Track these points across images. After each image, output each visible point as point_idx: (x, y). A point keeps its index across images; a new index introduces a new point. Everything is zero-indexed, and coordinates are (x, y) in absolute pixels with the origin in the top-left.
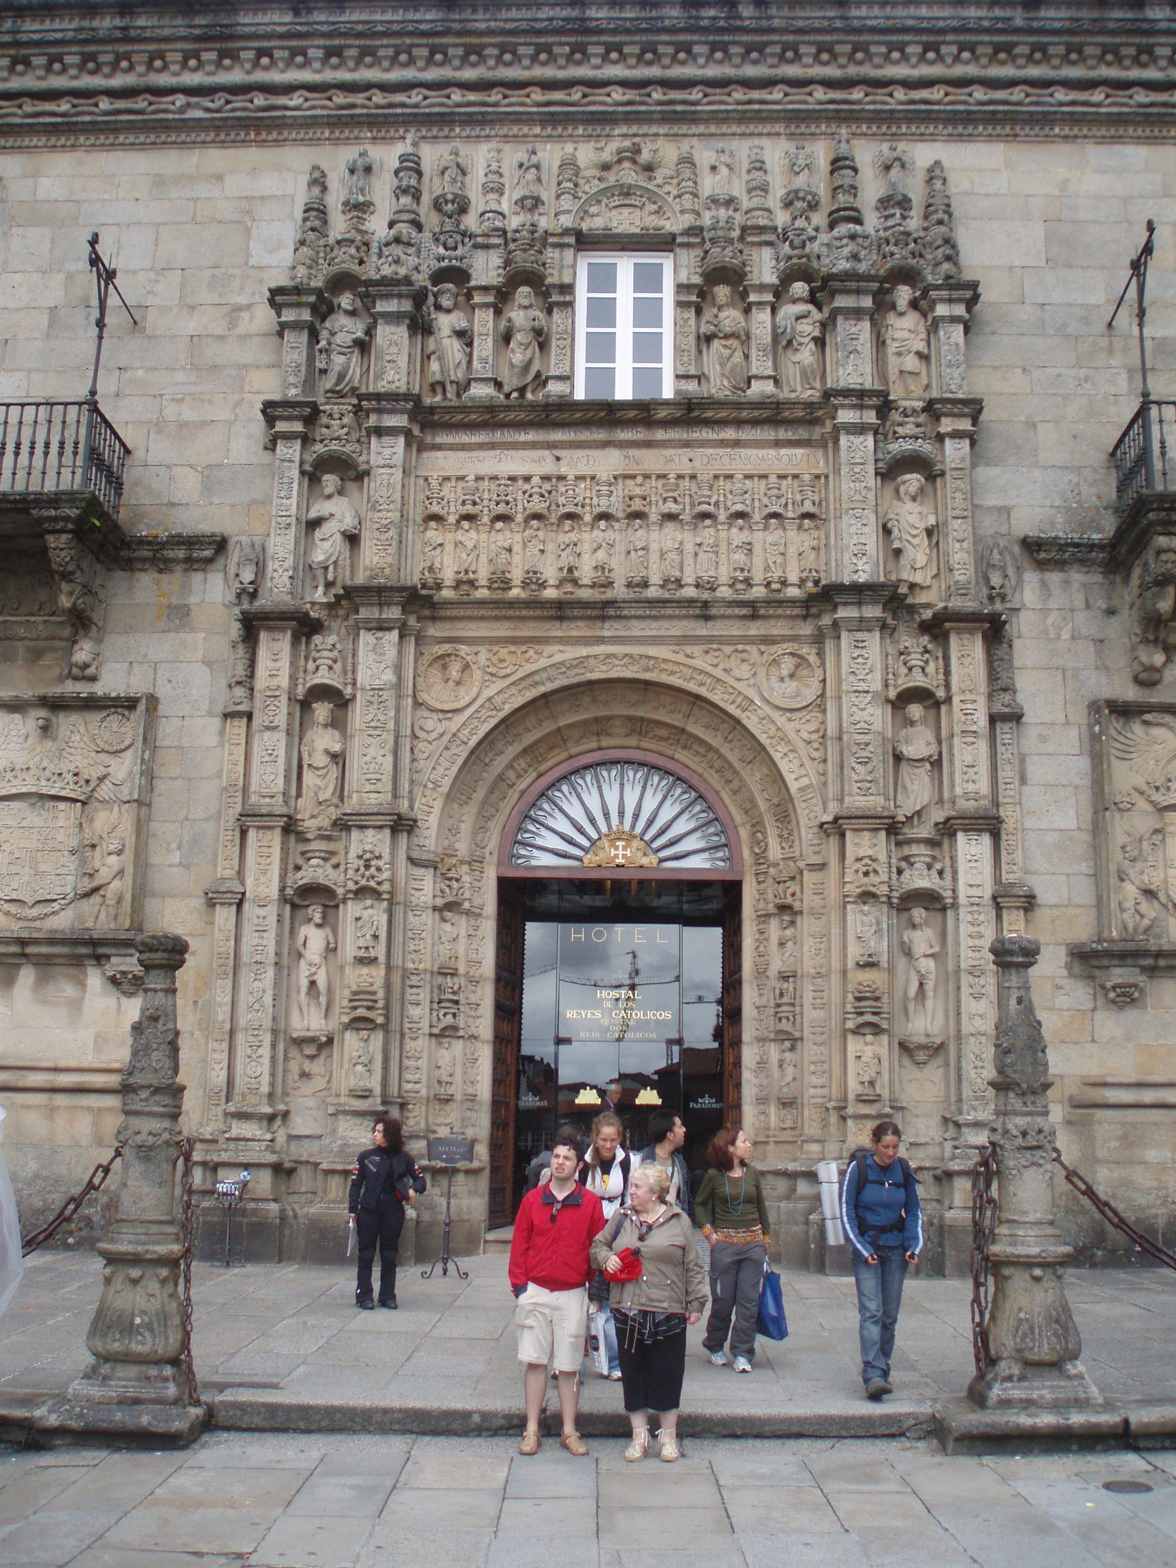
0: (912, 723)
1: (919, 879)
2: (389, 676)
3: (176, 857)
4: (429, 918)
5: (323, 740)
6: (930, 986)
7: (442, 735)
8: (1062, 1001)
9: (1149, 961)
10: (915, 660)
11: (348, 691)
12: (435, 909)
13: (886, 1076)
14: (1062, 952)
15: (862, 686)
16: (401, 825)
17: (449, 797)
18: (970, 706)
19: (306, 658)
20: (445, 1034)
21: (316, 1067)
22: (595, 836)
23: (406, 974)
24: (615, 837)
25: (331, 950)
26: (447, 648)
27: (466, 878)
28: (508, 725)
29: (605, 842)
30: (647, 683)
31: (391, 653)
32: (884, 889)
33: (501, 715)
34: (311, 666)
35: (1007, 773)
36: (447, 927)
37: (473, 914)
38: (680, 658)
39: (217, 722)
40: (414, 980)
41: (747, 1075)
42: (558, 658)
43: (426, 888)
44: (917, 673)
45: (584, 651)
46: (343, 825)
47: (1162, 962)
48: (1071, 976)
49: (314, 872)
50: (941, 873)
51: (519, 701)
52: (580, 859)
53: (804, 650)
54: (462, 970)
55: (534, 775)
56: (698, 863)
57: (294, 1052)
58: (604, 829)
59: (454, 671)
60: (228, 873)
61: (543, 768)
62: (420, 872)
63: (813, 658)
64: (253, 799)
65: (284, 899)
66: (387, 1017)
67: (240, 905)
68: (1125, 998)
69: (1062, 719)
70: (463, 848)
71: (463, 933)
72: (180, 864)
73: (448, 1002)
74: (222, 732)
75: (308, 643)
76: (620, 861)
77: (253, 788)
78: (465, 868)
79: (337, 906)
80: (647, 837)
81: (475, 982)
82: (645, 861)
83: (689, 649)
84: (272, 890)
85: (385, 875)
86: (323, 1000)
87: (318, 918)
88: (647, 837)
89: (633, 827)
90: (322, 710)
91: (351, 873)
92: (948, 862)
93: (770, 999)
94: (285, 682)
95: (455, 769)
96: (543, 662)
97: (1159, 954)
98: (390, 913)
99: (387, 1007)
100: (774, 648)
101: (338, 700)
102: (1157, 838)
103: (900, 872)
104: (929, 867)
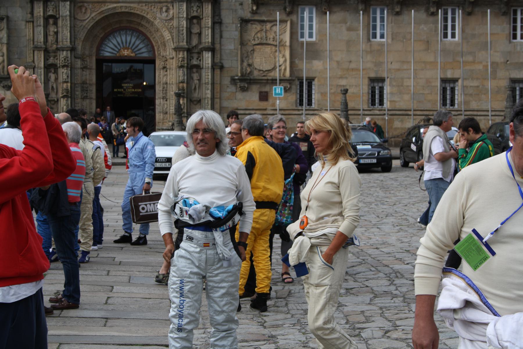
0: (194, 24)
1: (195, 62)
2: (68, 13)
3: (16, 57)
4: (79, 71)
5: (52, 29)
6: (197, 87)
7: (81, 26)
8: (229, 90)
9: (249, 81)
10: (195, 9)
11: (58, 16)
12: (81, 68)
13: (186, 107)
14: (229, 79)
15: (182, 16)
16: (73, 49)
17: (83, 41)
18: (208, 21)
19: (47, 7)
20: (84, 98)
21: (54, 106)
22: (119, 48)
23: (75, 84)
24: (125, 48)
25: (56, 79)
26: (81, 4)
27: (88, 60)
28: (97, 23)
29: (122, 50)
30: (131, 13)
31: (68, 7)
32: (186, 65)
33: (95, 21)
34: (48, 10)
35: (217, 36)
36: (84, 72)
37: (90, 69)
38: (139, 7)
39: (24, 23)
40: (77, 85)
41: (157, 106)
42: (109, 7)
43: (79, 63)
44: (195, 12)
45: (115, 5)
46: (58, 49)
47: (252, 81)
48: (231, 84)
49: (51, 61)
50: (200, 60)
51: (100, 17)
52: (116, 54)
53: (169, 5)
54: (88, 82)
55: (104, 34)
56: (145, 55)
57: (49, 103)
58: (122, 46)
59: (83, 10)
60: (30, 61)
61: (107, 31)
62: (77, 60)
63: (171, 7)
64: (36, 43)
65: (45, 67)
66: (71, 95)
67: (34, 69)
68: (243, 89)
69: (231, 22)
70: (87, 53)
71: (88, 73)
72: (18, 58)
73: (84, 90)
74: (26, 25)
75: (47, 3)
76: (126, 55)
77: (36, 40)
78: (88, 58)
79: (57, 69)
80: (133, 48)
81: (90, 85)
82: (132, 55)
83: (141, 5)
84: (42, 65)
85: (69, 62)
86: (55, 91)
87: (53, 71)
88: (133, 48)
89: (129, 46)
90: (51, 21)
91: (61, 61)
92: (202, 58)
93: (161, 89)
94: (42, 14)
95: (85, 34)
96: (106, 8)
97: (250, 80)
98: (71, 70)
99: (71, 93)
100: (161, 5)
101: (55, 18)
102: (252, 52)
103: (190, 60)
104: (197, 59)
